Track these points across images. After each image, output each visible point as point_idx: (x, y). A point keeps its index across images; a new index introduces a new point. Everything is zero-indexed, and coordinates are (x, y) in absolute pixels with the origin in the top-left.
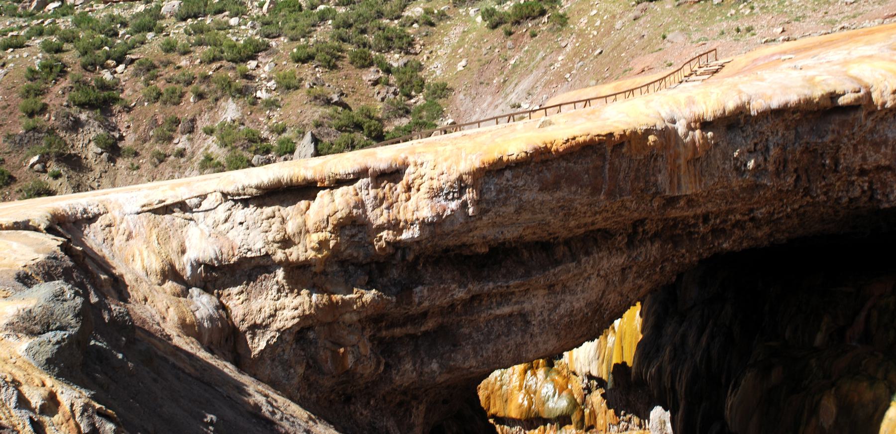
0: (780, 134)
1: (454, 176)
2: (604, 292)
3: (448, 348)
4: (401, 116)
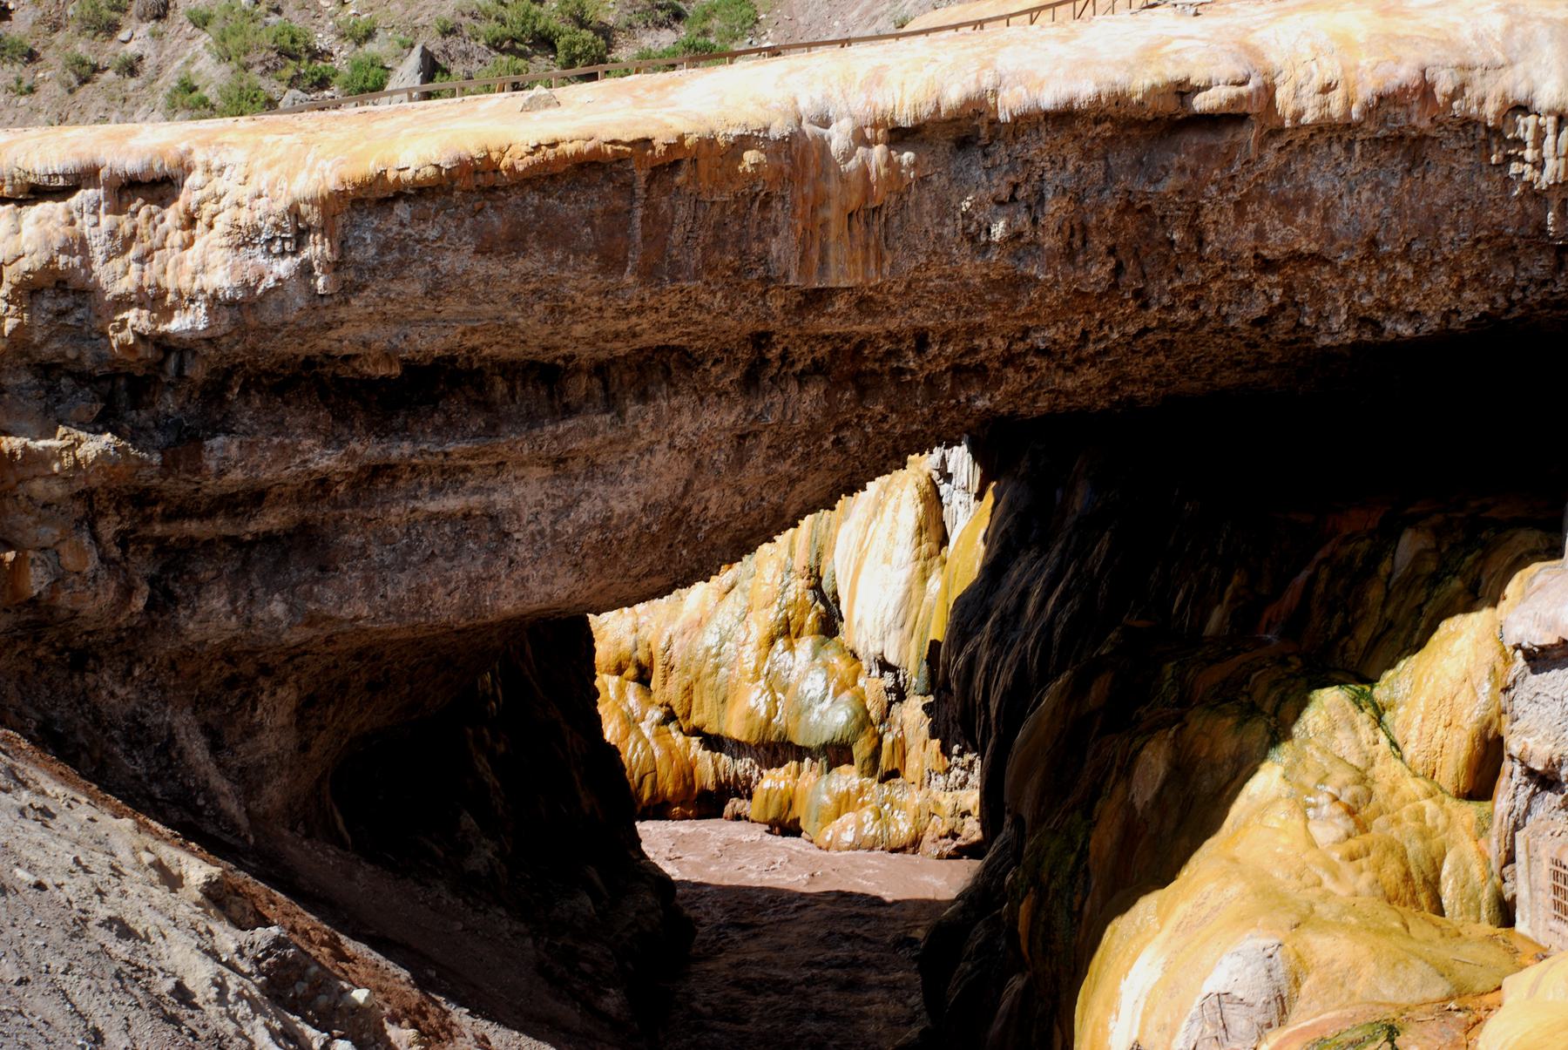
0: (1070, 167)
1: (281, 205)
2: (689, 484)
3: (309, 572)
4: (660, 25)
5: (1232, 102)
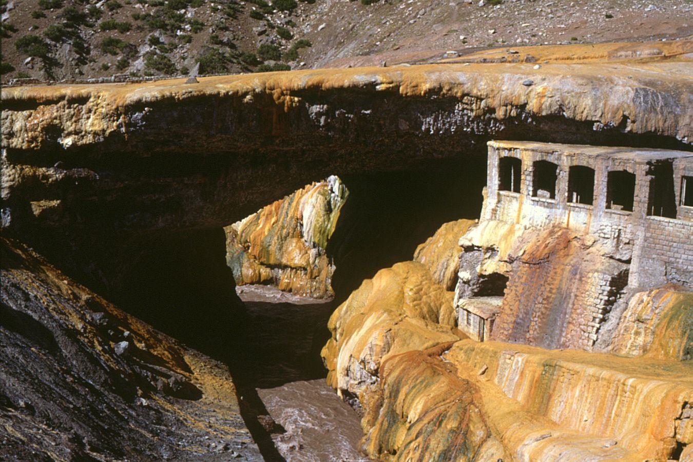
5: (388, 89)
